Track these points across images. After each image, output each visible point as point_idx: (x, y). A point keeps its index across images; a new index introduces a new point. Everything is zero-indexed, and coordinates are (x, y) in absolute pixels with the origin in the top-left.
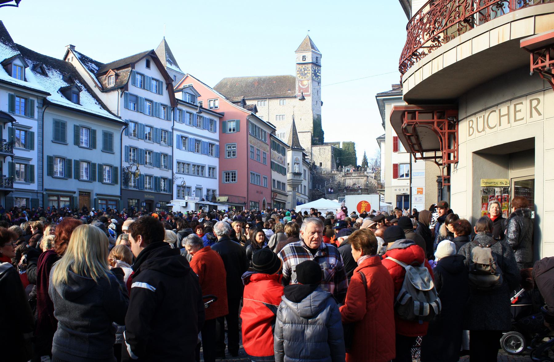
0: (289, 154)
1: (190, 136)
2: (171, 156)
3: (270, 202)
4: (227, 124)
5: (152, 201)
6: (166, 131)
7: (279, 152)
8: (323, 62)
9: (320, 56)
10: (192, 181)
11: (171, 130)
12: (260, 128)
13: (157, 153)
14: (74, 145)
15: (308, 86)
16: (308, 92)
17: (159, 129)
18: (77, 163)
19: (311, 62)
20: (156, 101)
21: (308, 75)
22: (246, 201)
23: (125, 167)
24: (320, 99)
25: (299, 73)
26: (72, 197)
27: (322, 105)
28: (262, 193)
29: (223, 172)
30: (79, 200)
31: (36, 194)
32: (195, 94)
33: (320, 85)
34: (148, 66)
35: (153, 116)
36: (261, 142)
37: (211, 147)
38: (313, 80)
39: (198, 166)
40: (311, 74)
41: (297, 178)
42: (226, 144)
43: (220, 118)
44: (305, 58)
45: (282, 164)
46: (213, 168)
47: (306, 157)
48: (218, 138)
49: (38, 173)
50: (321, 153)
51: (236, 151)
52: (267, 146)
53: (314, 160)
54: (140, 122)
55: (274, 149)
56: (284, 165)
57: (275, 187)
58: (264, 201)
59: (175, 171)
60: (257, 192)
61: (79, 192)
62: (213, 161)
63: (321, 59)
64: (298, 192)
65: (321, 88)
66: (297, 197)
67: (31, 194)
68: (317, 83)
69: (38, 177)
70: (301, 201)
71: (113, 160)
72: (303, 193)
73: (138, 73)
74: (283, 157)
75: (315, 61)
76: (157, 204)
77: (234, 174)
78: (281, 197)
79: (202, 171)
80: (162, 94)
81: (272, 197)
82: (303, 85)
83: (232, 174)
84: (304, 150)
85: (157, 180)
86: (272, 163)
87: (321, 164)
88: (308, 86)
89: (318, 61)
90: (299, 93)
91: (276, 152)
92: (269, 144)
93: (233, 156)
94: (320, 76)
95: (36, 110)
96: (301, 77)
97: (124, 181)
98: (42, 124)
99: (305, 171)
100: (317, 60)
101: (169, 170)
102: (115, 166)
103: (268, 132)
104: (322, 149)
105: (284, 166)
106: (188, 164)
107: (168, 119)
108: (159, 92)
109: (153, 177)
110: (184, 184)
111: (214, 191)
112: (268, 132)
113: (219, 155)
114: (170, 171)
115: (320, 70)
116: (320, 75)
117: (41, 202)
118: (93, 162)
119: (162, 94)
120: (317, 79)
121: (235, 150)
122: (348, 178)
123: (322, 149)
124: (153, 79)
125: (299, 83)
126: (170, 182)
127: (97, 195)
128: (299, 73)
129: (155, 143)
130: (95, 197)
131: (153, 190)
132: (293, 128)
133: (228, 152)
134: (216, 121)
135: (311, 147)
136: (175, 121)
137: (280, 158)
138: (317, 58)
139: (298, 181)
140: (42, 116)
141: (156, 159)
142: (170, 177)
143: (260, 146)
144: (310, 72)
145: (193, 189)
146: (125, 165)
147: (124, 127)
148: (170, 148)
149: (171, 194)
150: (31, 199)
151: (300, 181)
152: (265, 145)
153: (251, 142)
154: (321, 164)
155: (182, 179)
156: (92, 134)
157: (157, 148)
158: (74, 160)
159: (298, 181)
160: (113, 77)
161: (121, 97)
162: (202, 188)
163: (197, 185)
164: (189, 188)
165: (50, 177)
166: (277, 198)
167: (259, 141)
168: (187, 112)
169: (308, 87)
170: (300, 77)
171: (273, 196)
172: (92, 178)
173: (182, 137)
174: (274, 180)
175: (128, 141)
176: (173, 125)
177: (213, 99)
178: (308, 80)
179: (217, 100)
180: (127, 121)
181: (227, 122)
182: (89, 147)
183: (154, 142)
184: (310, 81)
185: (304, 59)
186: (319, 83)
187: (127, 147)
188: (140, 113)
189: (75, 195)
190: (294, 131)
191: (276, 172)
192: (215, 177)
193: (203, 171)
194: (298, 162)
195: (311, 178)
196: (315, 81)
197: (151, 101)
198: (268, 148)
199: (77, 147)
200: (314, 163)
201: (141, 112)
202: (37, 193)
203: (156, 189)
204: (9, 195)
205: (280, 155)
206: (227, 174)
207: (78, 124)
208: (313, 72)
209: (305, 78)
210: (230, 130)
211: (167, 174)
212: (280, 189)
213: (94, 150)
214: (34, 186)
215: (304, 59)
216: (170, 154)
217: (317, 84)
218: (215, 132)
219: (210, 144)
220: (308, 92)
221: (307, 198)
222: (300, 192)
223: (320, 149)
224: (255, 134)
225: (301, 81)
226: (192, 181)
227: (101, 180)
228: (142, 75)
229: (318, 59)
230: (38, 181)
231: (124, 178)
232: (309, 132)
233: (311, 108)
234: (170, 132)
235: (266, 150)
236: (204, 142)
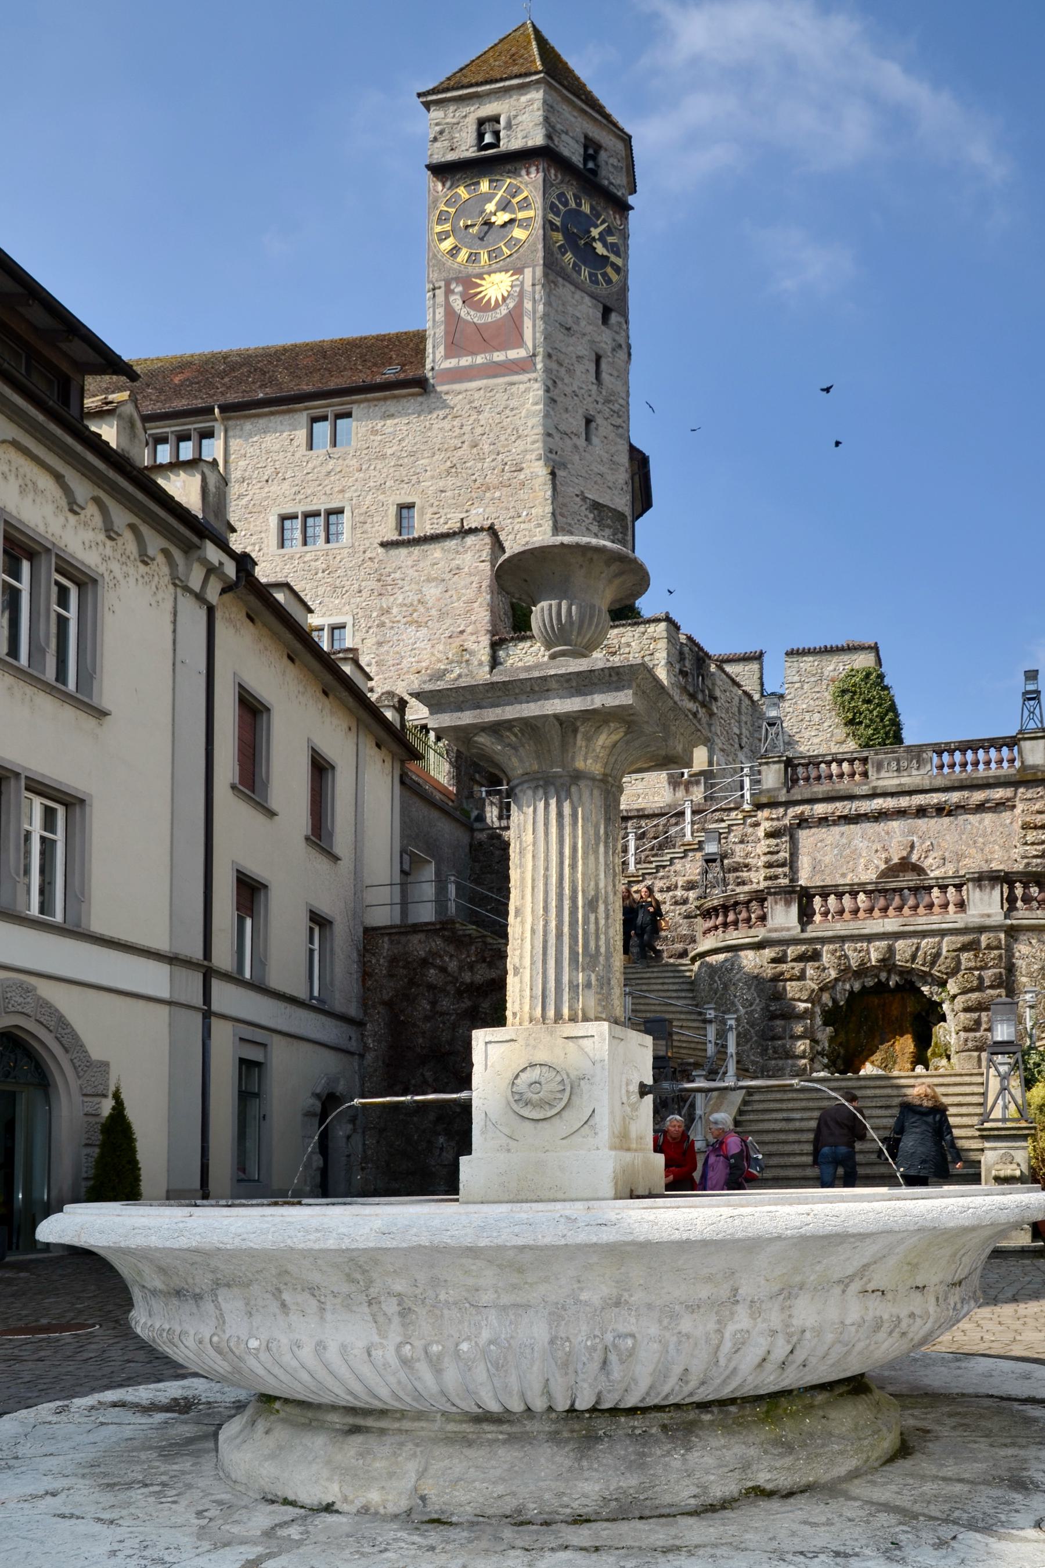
15: (520, 305)
16: (520, 343)
21: (519, 233)
38: (551, 266)
40: (539, 222)
44: (497, 134)
90: (448, 356)
96: (463, 255)
122: (820, 809)
125: (449, 292)
128: (447, 227)
144: (534, 213)
169: (515, 318)
170: (454, 251)
184: (532, 275)
215: (488, 139)
217: (586, 309)
220: (520, 343)
225: (469, 282)
233: (539, 448)
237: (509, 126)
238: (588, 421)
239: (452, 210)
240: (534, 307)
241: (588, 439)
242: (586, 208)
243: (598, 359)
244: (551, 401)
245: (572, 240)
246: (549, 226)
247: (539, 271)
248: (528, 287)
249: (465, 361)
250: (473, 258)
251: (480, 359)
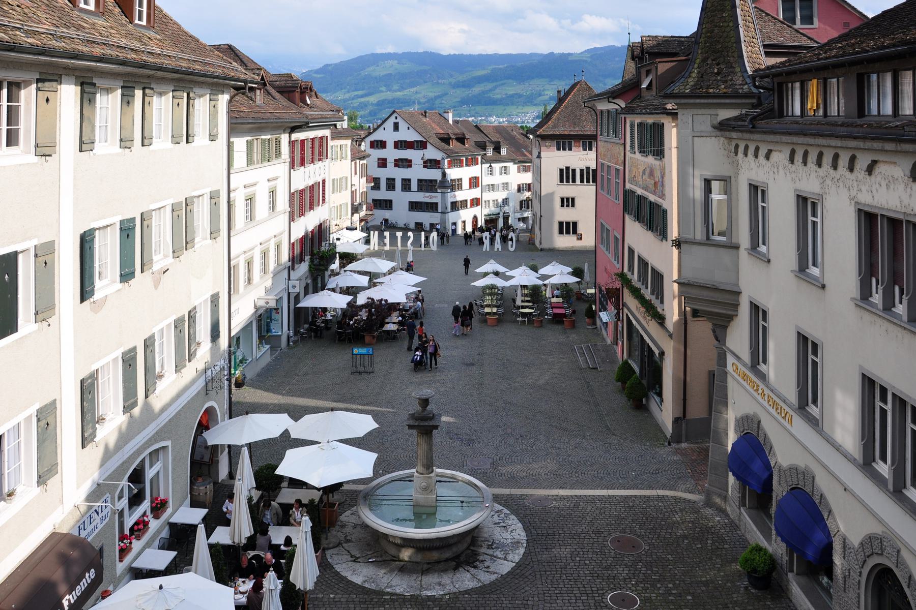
45: (654, 193)
56: (662, 196)
74: (657, 163)
105: (659, 201)
137: (647, 173)
205: (651, 160)
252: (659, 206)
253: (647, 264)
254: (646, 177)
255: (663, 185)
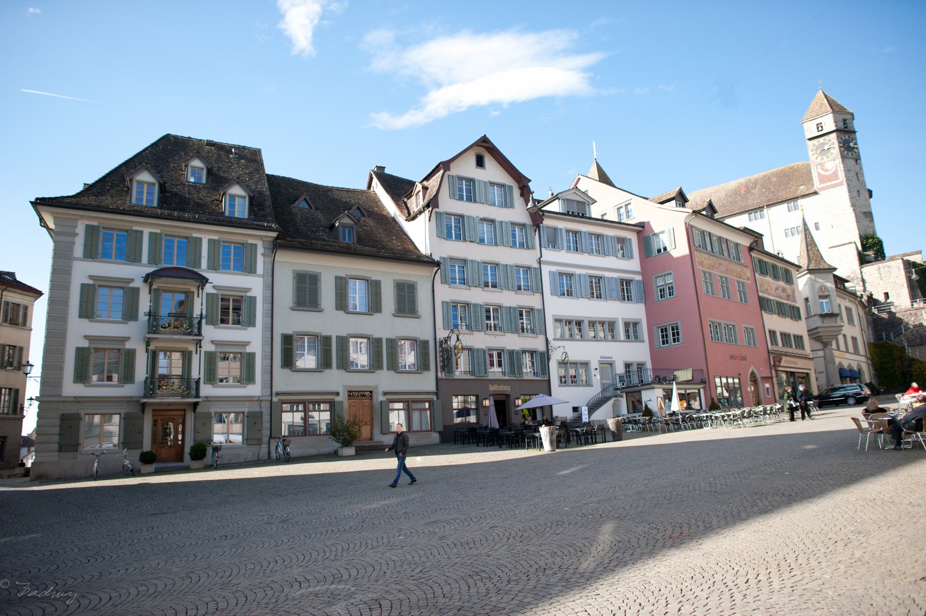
0: (802, 282)
1: (578, 271)
2: (541, 310)
3: (769, 375)
4: (652, 240)
5: (508, 396)
6: (528, 269)
7: (776, 277)
8: (857, 125)
9: (851, 116)
10: (577, 350)
11: (536, 265)
12: (723, 238)
13: (510, 308)
14: (337, 309)
15: (836, 168)
17: (511, 266)
18: (343, 342)
19: (834, 128)
20: (500, 220)
22: (706, 377)
23: (442, 339)
24: (865, 186)
25: (814, 152)
26: (333, 403)
27: (871, 196)
28: (744, 359)
29: (655, 327)
30: (350, 406)
31: (257, 403)
32: (584, 201)
33: (860, 163)
34: (480, 162)
35: (496, 244)
36: (727, 263)
37: (627, 286)
38: (843, 157)
39: (602, 323)
41: (828, 322)
42: (654, 276)
43: (639, 233)
44: (822, 127)
45: (788, 300)
46: (635, 324)
47: (847, 285)
48: (639, 269)
49: (263, 366)
50: (883, 276)
51: (673, 285)
52: (745, 269)
53: (871, 290)
54: (470, 258)
55: (763, 272)
56: (795, 301)
57: (777, 344)
58: (753, 374)
59: (550, 336)
60: (732, 357)
61: (349, 391)
62: (635, 311)
63: (854, 121)
64: (838, 349)
65: (863, 167)
66: (837, 361)
67: (247, 404)
68: (852, 160)
69: (263, 373)
70: (850, 365)
71: (420, 328)
72: (851, 349)
73: (461, 178)
75: (841, 125)
76: (517, 401)
77: (675, 329)
78: (796, 363)
79: (635, 332)
80: (512, 206)
81: (772, 364)
82: (826, 171)
83: (673, 329)
84: (835, 269)
85: (514, 357)
86: (761, 300)
87: (887, 295)
88: (836, 170)
89: (849, 126)
90: (820, 184)
91: (768, 279)
92: (750, 265)
93: (670, 295)
94: (857, 148)
95: (260, 260)
97: (442, 364)
98: (271, 282)
99: (849, 310)
100: (844, 124)
101: (539, 336)
102: (422, 339)
103: (746, 242)
104: (884, 267)
105: (793, 304)
106: (579, 323)
107: (525, 245)
108: (507, 203)
109: (505, 351)
110: (566, 357)
111: (641, 366)
112: (746, 242)
113: (646, 298)
114: (541, 338)
115: (856, 138)
116: (856, 146)
117: (266, 418)
118: (376, 336)
119: (512, 206)
120: (852, 154)
121: (672, 283)
123: (884, 267)
124: (492, 184)
125: (817, 168)
126: (542, 359)
127: (385, 394)
129: (504, 291)
130: (382, 398)
131: (507, 375)
132: (806, 235)
133: (661, 290)
134: (630, 240)
135: (860, 269)
136: (542, 249)
137: (780, 289)
138: (845, 121)
139: (834, 329)
140: (271, 269)
141: (509, 318)
142: (542, 348)
143: (727, 270)
144: (836, 145)
145: (594, 364)
146: (442, 334)
147: (436, 269)
148: (538, 296)
149: (547, 379)
150: (248, 412)
151: (837, 329)
152: (738, 269)
153: (701, 264)
154: (887, 295)
155: (561, 350)
156: (374, 288)
157: (508, 299)
158: (337, 336)
159: (834, 329)
160: (421, 194)
161: (430, 221)
162: (614, 361)
163: (601, 357)
164: (586, 364)
165: (287, 371)
166: (782, 364)
167: (722, 261)
168: (568, 231)
170: (817, 158)
171: (774, 362)
172: (376, 364)
173: (561, 274)
174: (773, 333)
175: (446, 293)
176: (539, 256)
177: (623, 205)
178: (834, 160)
179: (630, 203)
180: (444, 259)
181: (651, 237)
182: (369, 311)
183: (502, 289)
184: (839, 160)
185: (819, 126)
186: (856, 160)
187: (447, 303)
188: (471, 243)
189: (337, 399)
190: (809, 240)
191: (775, 317)
192: (641, 340)
193: (612, 330)
194: (826, 293)
195: (868, 323)
196: (848, 158)
197: (492, 221)
198: (748, 273)
199: (341, 313)
200: (871, 295)
201: (471, 241)
202: (261, 401)
203: (512, 372)
204: (199, 409)
205: (782, 284)
206: (664, 330)
207: (343, 275)
208: (841, 145)
209: (828, 157)
210: (659, 251)
211: (537, 344)
212: (791, 347)
213: (377, 315)
214: (255, 390)
215: (820, 129)
216: (538, 306)
217: (852, 162)
218: (631, 257)
219: (622, 281)
220: (837, 178)
221: (863, 359)
222: (842, 347)
223: (879, 268)
224: (709, 248)
225: (821, 165)
226: (577, 350)
227: (394, 366)
228: (471, 181)
229: (848, 121)
230: (263, 380)
231: (441, 359)
232: (850, 243)
234: (535, 269)
235: (743, 276)
236: (608, 278)
237: (825, 125)
238: (858, 191)
239: (814, 148)
240: (841, 168)
241: (859, 196)
242: (847, 138)
243: (857, 174)
244: (849, 191)
245: (846, 149)
246: (840, 147)
247: (840, 159)
248: (838, 164)
249: (825, 185)
250: (822, 159)
251: (829, 184)
252: (794, 307)
253: (789, 335)
254: (780, 291)
255: (794, 297)
